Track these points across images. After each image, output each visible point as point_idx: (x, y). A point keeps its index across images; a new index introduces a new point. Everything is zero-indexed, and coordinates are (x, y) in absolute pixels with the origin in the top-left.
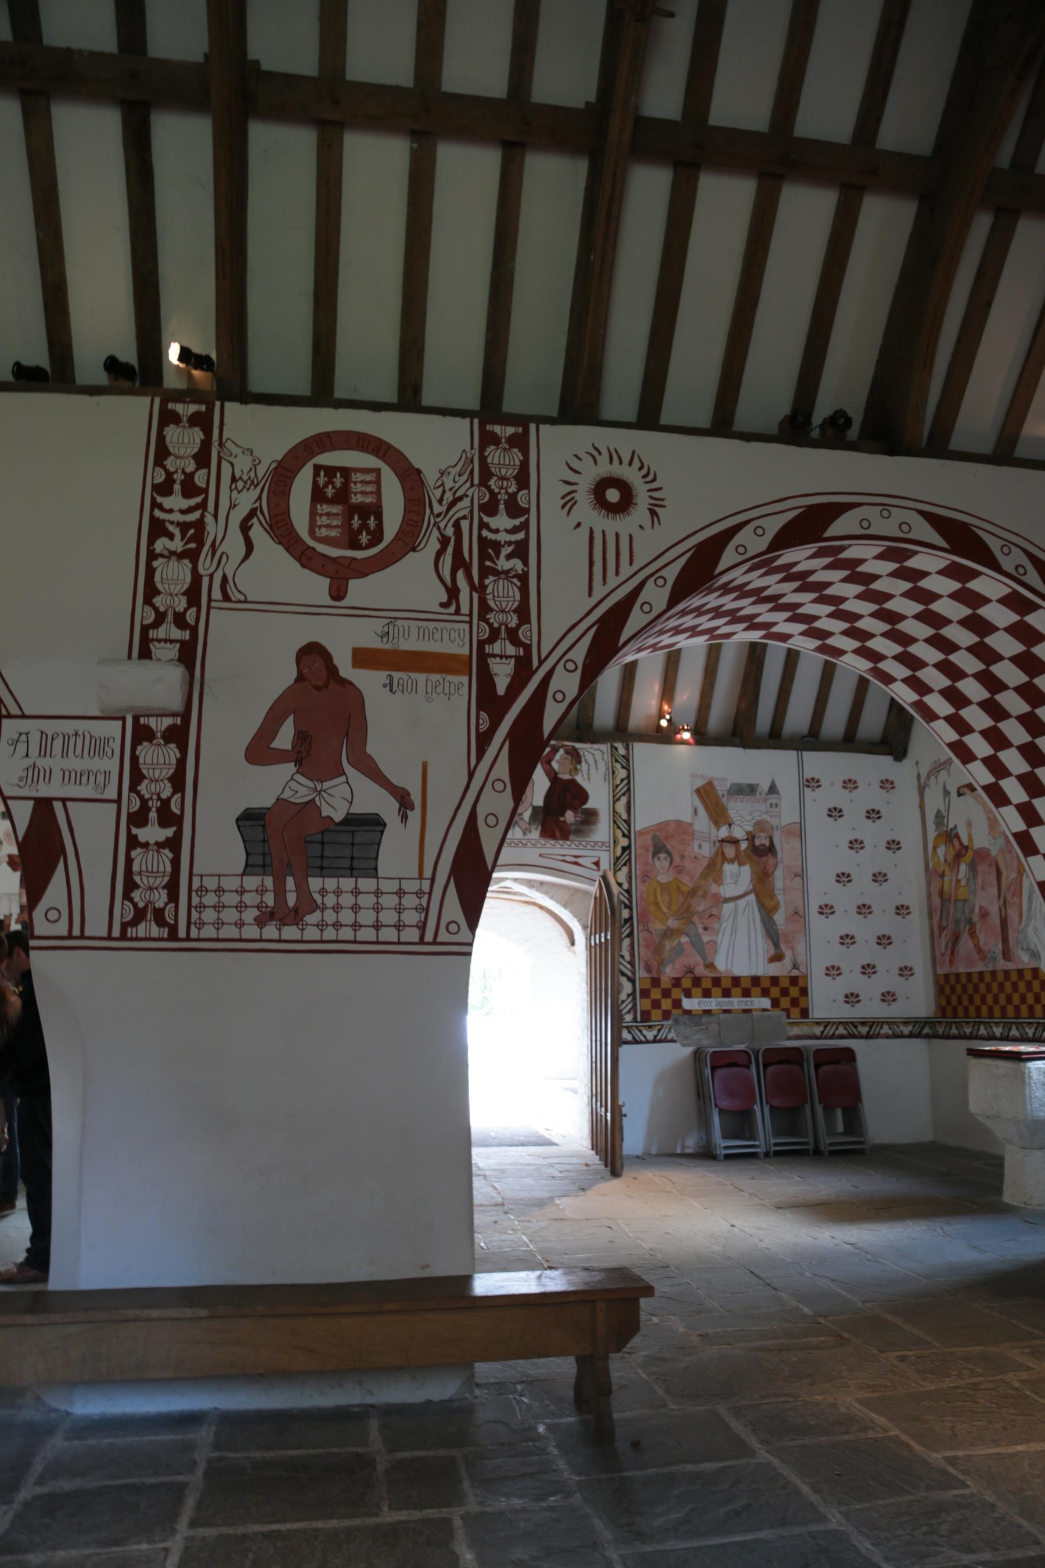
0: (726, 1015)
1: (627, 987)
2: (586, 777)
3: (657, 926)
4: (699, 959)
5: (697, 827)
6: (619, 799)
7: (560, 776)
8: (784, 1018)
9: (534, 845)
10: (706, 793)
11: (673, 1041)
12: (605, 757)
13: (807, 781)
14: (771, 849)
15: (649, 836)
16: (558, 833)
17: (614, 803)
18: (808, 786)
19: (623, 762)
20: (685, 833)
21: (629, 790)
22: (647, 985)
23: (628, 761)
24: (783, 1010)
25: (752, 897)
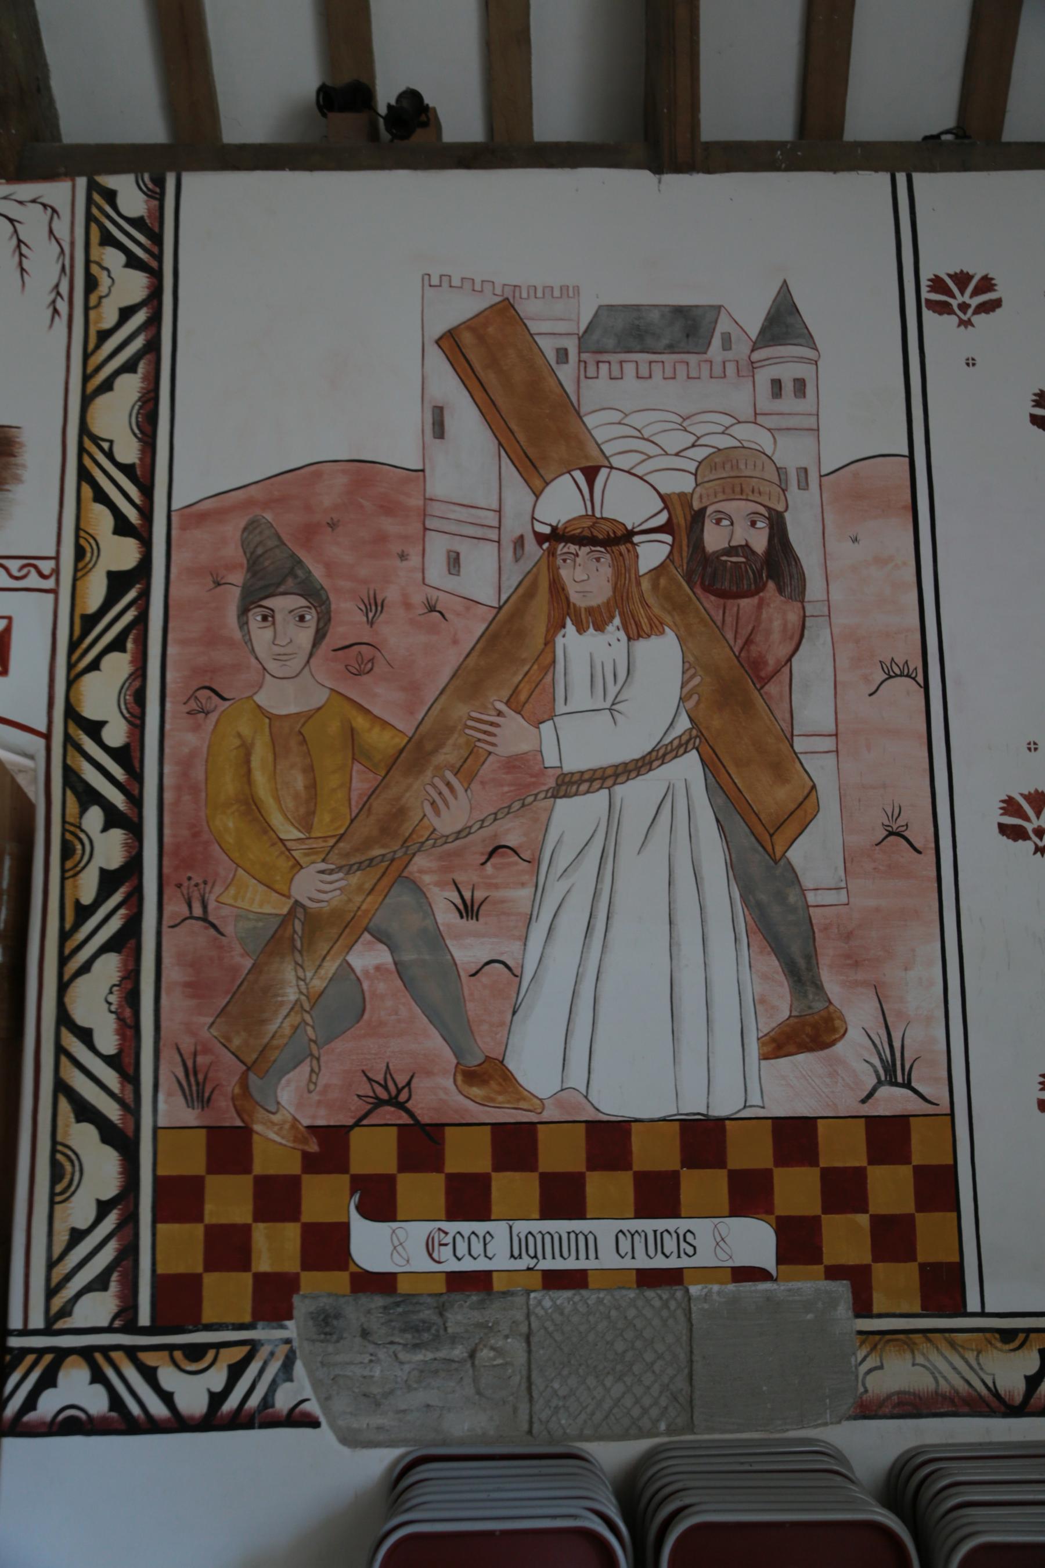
0: (563, 1297)
1: (101, 1170)
3: (246, 902)
4: (435, 1043)
5: (441, 484)
6: (107, 386)
8: (844, 1310)
11: (298, 1419)
12: (62, 228)
13: (938, 284)
14: (779, 565)
15: (233, 528)
17: (86, 401)
18: (942, 308)
19: (138, 245)
20: (389, 508)
21: (153, 347)
22: (192, 1161)
23: (157, 239)
24: (834, 1273)
25: (688, 768)
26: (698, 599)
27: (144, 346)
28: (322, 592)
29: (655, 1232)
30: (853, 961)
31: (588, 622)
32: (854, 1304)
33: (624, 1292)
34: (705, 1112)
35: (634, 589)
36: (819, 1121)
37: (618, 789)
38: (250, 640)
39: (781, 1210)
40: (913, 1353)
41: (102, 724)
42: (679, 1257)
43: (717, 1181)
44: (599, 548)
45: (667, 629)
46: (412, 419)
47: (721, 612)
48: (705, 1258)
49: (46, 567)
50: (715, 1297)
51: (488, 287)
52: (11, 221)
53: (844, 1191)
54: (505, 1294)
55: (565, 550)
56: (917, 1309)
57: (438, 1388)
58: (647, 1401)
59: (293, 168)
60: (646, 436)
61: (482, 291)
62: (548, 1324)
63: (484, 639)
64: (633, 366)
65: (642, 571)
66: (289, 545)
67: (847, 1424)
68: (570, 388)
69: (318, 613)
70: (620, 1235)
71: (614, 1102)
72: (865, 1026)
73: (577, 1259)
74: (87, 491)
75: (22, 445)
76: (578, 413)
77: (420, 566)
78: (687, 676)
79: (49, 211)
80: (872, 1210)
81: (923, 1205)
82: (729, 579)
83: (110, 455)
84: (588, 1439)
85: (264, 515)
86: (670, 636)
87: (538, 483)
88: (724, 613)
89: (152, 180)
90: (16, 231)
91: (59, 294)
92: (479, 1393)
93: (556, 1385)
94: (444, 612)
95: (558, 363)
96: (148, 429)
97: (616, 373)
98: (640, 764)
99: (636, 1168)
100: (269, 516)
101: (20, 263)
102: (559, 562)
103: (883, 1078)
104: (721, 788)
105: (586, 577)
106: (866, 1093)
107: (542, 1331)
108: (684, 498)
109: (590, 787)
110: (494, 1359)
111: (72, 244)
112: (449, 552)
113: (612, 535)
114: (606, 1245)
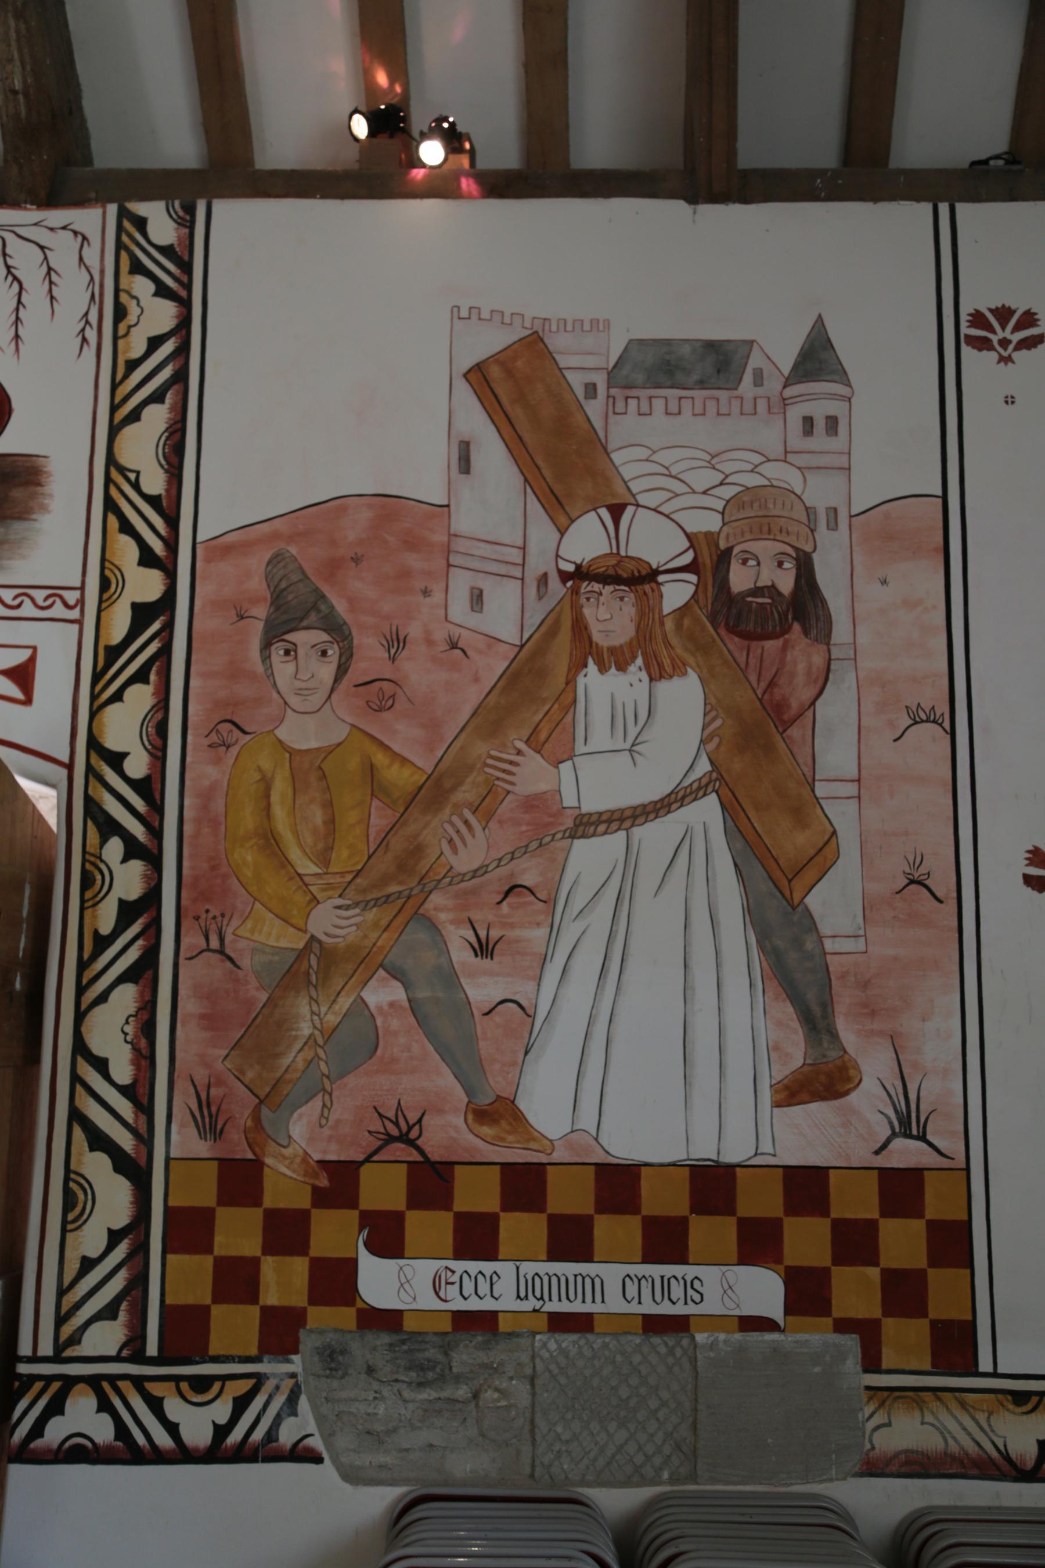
0: (569, 1340)
1: (113, 1199)
3: (263, 935)
4: (446, 1081)
5: (466, 520)
6: (135, 416)
8: (852, 1363)
10: (523, 395)
11: (302, 1454)
12: (91, 255)
13: (978, 319)
15: (257, 562)
17: (114, 431)
18: (982, 344)
19: (167, 272)
20: (413, 543)
21: (181, 377)
22: (203, 1193)
23: (187, 267)
24: (842, 1326)
25: (707, 810)
26: (722, 640)
27: (172, 376)
28: (344, 627)
29: (662, 1277)
30: (870, 1010)
31: (610, 662)
32: (863, 1358)
33: (630, 1338)
34: (715, 1158)
35: (657, 629)
36: (831, 1171)
37: (637, 831)
38: (272, 673)
39: (788, 1261)
40: (922, 1411)
41: (124, 755)
42: (686, 1303)
43: (726, 1229)
44: (623, 587)
45: (689, 670)
46: (438, 454)
47: (745, 653)
48: (712, 1305)
49: (72, 597)
50: (721, 1345)
51: (517, 320)
52: (42, 248)
53: (855, 1243)
54: (510, 1335)
55: (589, 588)
56: (928, 1367)
57: (441, 1427)
58: (650, 1449)
59: (324, 197)
60: (673, 474)
61: (511, 324)
62: (553, 1367)
63: (505, 677)
64: (662, 401)
65: (665, 612)
66: (313, 579)
67: (853, 1482)
68: (598, 425)
69: (340, 648)
70: (627, 1280)
71: (623, 1146)
72: (881, 1077)
73: (584, 1302)
74: (113, 522)
75: (49, 474)
76: (605, 449)
77: (443, 602)
78: (708, 718)
79: (80, 238)
80: (884, 1263)
81: (935, 1261)
82: (754, 620)
83: (136, 486)
84: (589, 1485)
85: (289, 549)
86: (693, 677)
87: (563, 520)
88: (748, 655)
89: (183, 207)
90: (46, 258)
91: (87, 322)
92: (483, 1435)
93: (559, 1429)
94: (465, 649)
95: (586, 398)
96: (175, 460)
97: (645, 409)
98: (659, 806)
99: (645, 1212)
100: (293, 550)
101: (50, 290)
102: (583, 600)
103: (897, 1130)
104: (740, 832)
105: (608, 616)
106: (879, 1145)
107: (547, 1374)
108: (711, 537)
109: (608, 827)
110: (498, 1400)
111: (102, 272)
112: (472, 589)
113: (637, 574)
114: (613, 1289)
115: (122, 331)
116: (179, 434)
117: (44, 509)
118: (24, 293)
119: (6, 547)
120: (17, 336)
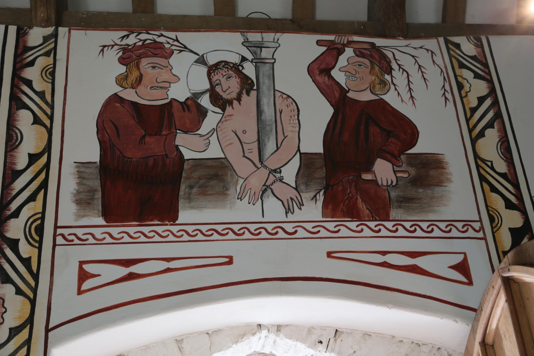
2: (406, 96)
6: (481, 134)
7: (350, 95)
9: (314, 234)
16: (362, 206)
17: (474, 142)
21: (498, 115)
49: (477, 226)
52: (413, 56)
74: (486, 187)
75: (447, 163)
79: (430, 52)
83: (492, 168)
90: (416, 61)
91: (445, 90)
96: (508, 155)
101: (423, 76)
111: (446, 67)
115: (463, 94)
116: (506, 143)
117: (449, 180)
118: (410, 77)
119: (434, 200)
120: (412, 97)
